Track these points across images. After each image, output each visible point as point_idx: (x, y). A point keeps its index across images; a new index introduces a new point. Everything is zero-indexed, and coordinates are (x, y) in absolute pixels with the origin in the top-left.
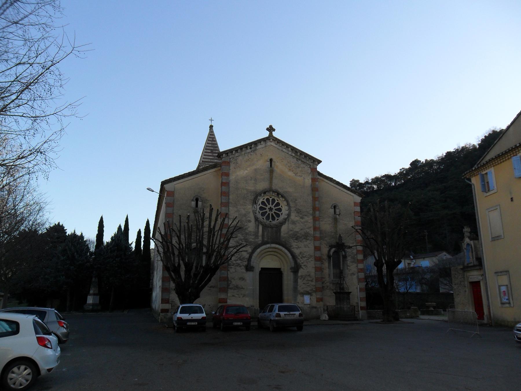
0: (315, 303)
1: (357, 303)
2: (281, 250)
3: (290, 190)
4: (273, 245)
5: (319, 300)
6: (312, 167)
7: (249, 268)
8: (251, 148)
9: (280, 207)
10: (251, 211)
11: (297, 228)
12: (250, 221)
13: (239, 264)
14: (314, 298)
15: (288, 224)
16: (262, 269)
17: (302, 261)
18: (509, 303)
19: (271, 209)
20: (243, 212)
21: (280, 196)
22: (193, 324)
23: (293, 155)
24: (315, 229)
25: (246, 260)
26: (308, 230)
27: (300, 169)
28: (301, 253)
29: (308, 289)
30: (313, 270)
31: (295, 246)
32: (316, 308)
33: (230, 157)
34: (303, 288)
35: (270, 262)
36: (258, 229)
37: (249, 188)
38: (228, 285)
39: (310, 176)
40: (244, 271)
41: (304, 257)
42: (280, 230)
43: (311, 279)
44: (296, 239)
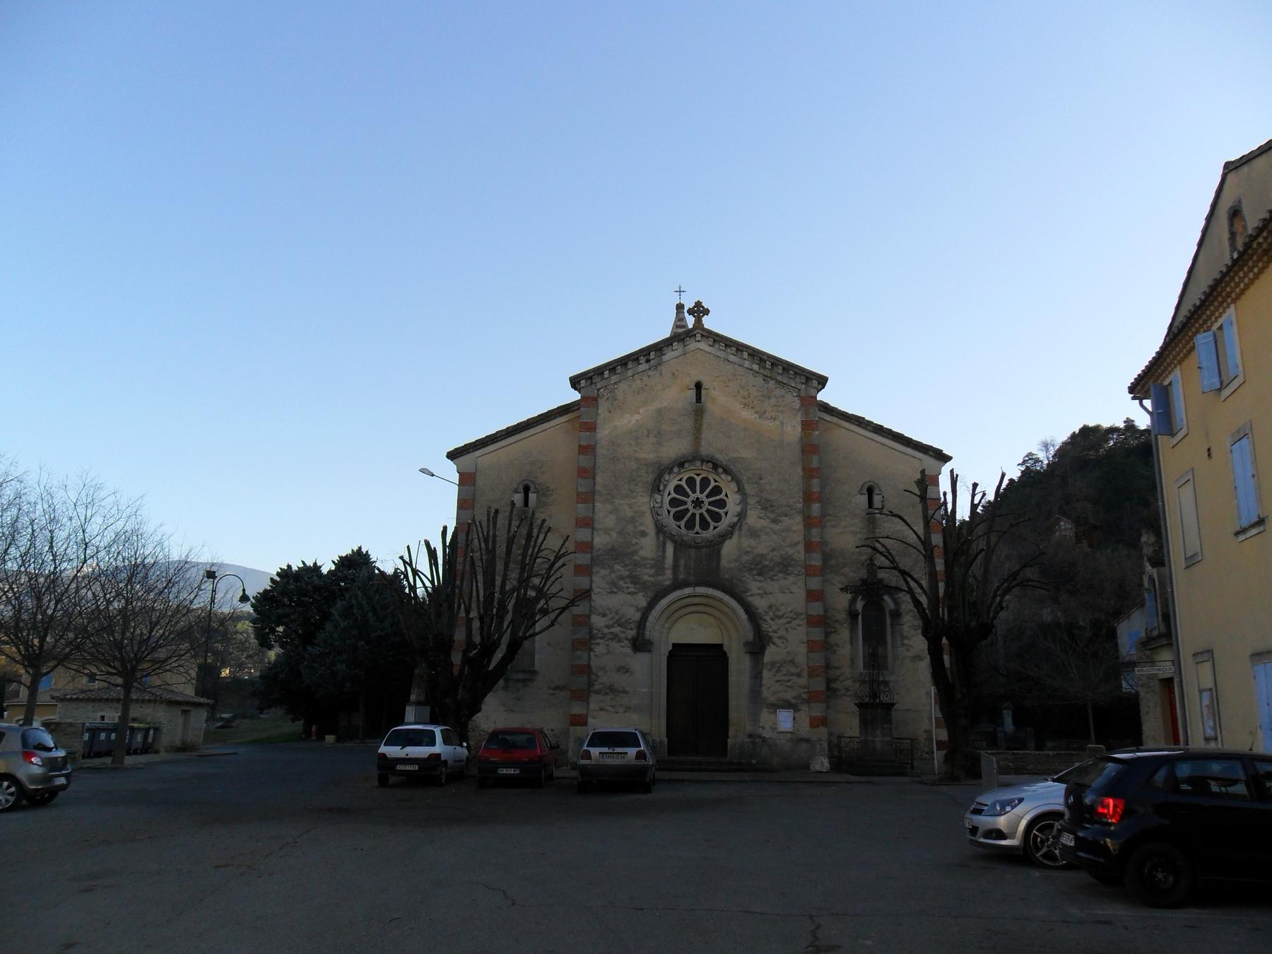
0: (805, 730)
1: (929, 732)
2: (720, 600)
3: (747, 454)
4: (701, 590)
5: (815, 723)
6: (803, 394)
7: (641, 644)
8: (648, 361)
9: (722, 496)
10: (646, 508)
11: (762, 547)
12: (644, 534)
13: (616, 635)
14: (804, 716)
15: (740, 537)
16: (676, 646)
17: (774, 628)
18: (1216, 739)
19: (698, 503)
20: (629, 513)
21: (720, 470)
22: (409, 768)
23: (755, 367)
24: (809, 547)
25: (633, 625)
26: (791, 551)
27: (773, 401)
28: (770, 607)
29: (789, 695)
30: (803, 649)
31: (755, 591)
32: (807, 741)
33: (599, 386)
34: (775, 693)
35: (695, 631)
36: (664, 551)
37: (642, 455)
38: (590, 684)
39: (799, 418)
40: (629, 651)
41: (779, 617)
42: (719, 551)
43: (797, 671)
44: (760, 574)
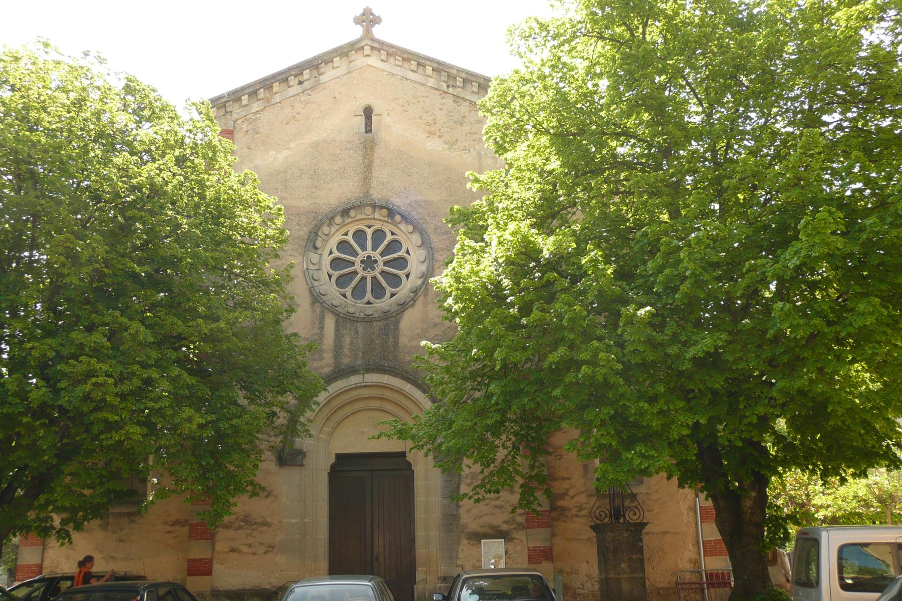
2: (400, 392)
9: (402, 253)
16: (339, 457)
19: (369, 263)
21: (398, 218)
27: (467, 128)
33: (235, 116)
36: (322, 328)
42: (397, 324)
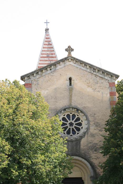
2: (81, 161)
6: (110, 82)
9: (80, 121)
15: (87, 137)
19: (71, 124)
21: (79, 111)
27: (99, 85)
33: (32, 80)
42: (80, 142)
44: (95, 151)
